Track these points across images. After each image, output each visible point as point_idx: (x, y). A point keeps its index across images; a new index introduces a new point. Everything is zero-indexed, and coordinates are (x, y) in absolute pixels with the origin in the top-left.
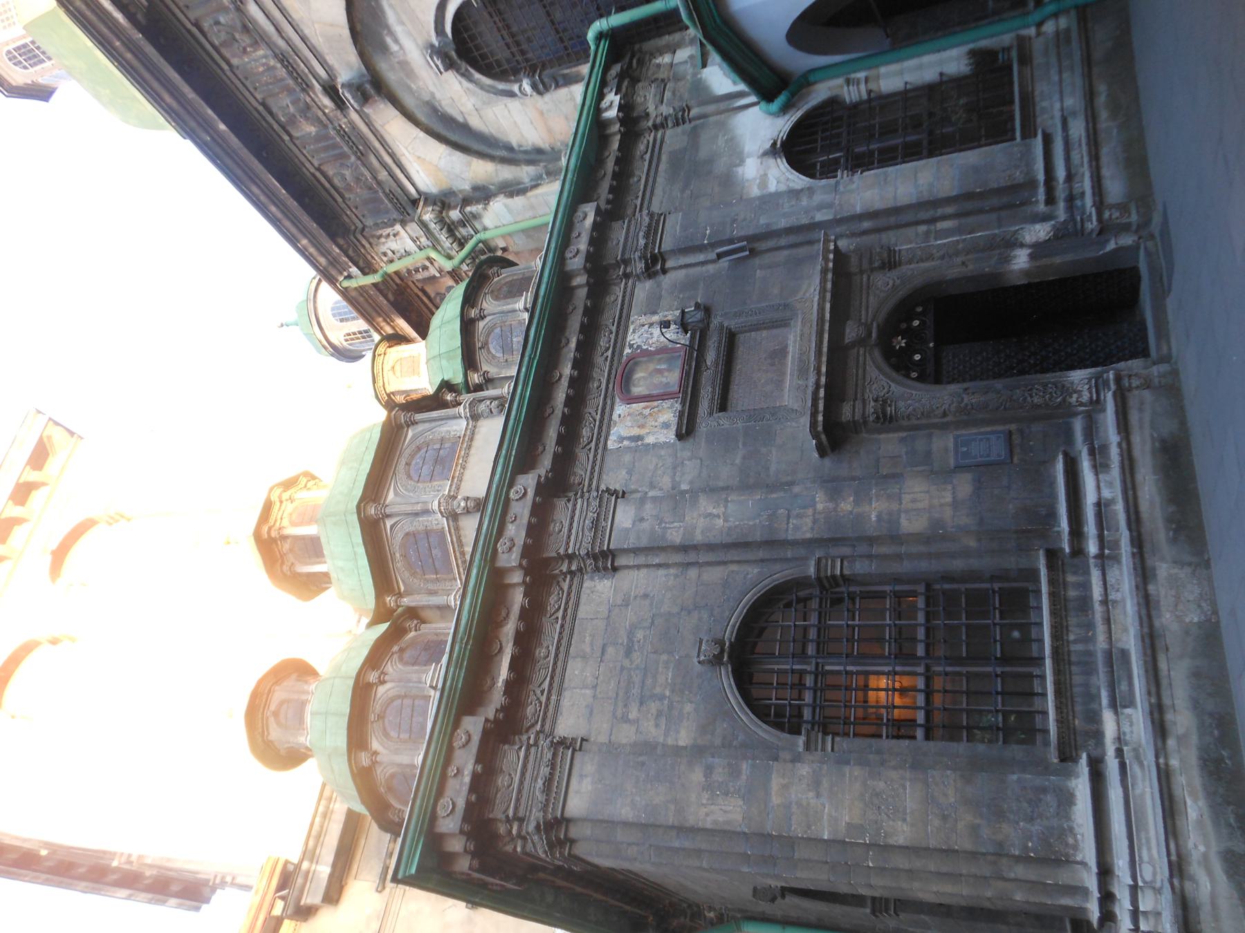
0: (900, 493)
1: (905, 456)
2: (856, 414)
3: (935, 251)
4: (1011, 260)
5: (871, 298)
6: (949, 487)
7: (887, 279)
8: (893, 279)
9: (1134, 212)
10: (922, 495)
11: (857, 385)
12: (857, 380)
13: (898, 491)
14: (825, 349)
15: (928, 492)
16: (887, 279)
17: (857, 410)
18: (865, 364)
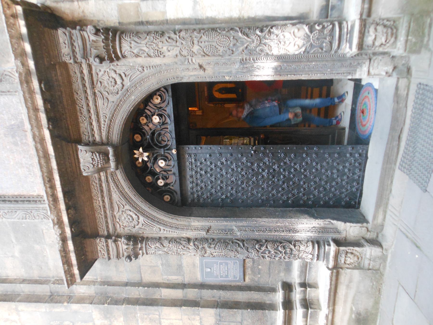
0: (160, 319)
1: (161, 267)
2: (111, 253)
3: (165, 48)
4: (253, 71)
5: (100, 102)
6: (198, 318)
7: (114, 75)
8: (120, 75)
9: (402, 38)
10: (177, 321)
11: (106, 217)
12: (105, 212)
13: (157, 316)
14: (60, 195)
15: (181, 320)
16: (114, 75)
17: (111, 249)
18: (109, 191)
